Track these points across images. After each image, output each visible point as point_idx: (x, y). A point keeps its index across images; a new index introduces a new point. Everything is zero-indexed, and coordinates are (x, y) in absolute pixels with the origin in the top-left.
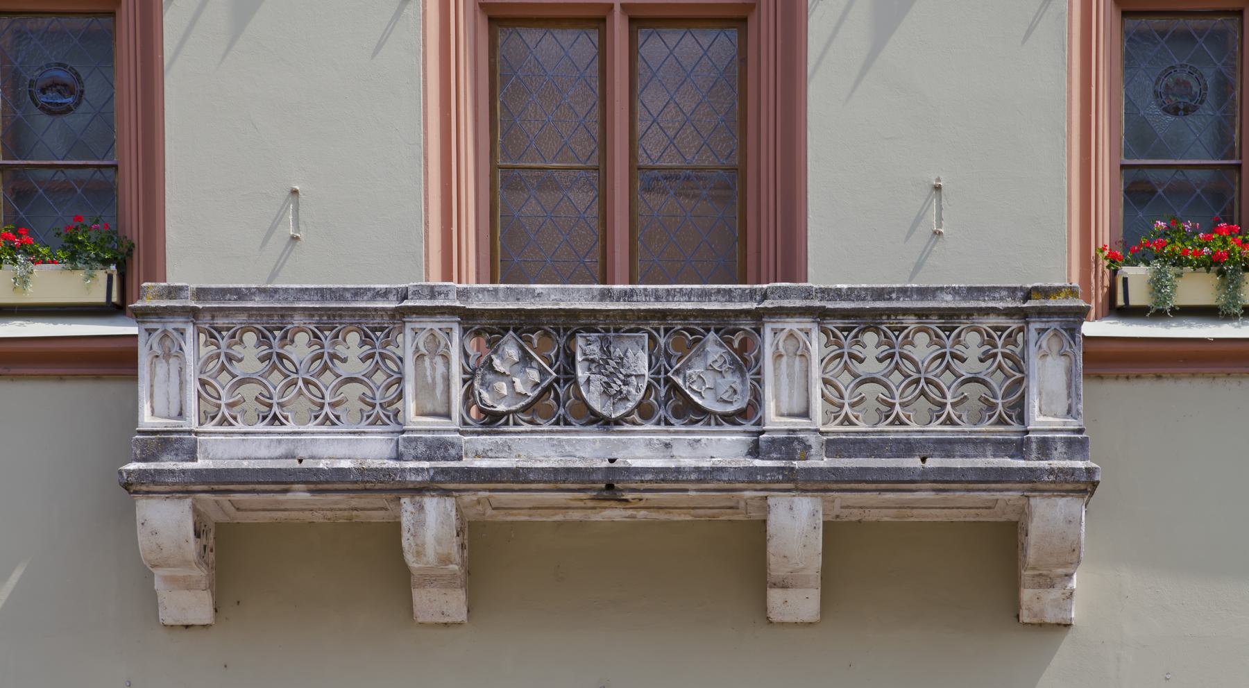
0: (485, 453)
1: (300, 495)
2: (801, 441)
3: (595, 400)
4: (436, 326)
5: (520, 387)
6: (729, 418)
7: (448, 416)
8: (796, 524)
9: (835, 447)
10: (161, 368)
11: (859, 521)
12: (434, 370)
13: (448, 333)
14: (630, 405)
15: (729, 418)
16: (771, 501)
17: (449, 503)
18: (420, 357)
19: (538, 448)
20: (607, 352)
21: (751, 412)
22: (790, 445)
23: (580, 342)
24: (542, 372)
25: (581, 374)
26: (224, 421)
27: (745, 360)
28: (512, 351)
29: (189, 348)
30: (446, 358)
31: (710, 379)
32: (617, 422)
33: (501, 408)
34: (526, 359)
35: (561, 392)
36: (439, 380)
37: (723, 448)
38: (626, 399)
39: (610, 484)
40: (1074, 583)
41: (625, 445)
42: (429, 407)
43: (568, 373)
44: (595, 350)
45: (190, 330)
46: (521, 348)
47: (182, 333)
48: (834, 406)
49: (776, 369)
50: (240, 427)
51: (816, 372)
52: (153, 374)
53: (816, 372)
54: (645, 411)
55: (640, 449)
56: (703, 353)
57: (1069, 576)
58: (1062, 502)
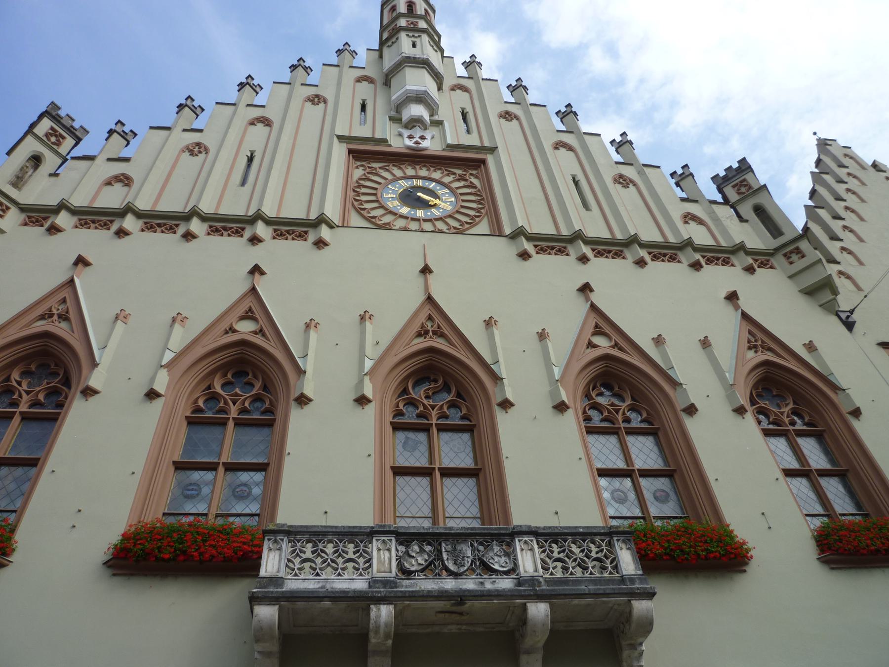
0: (407, 585)
1: (327, 604)
2: (537, 580)
3: (452, 567)
4: (386, 539)
5: (420, 560)
6: (505, 573)
7: (391, 572)
8: (539, 611)
9: (548, 581)
10: (272, 554)
11: (816, 249)
12: (384, 558)
13: (391, 540)
14: (466, 568)
15: (505, 573)
16: (528, 605)
17: (391, 607)
18: (379, 550)
19: (428, 585)
20: (455, 549)
21: (514, 570)
22: (533, 581)
23: (443, 545)
24: (429, 556)
25: (445, 556)
26: (296, 575)
27: (510, 554)
28: (416, 548)
29: (284, 546)
30: (389, 550)
31: (496, 559)
32: (461, 574)
33: (413, 569)
34: (422, 551)
35: (437, 564)
36: (387, 559)
37: (506, 584)
38: (463, 566)
39: (460, 597)
40: (644, 648)
41: (465, 584)
42: (382, 569)
43: (439, 557)
44: (449, 548)
45: (285, 539)
46: (420, 547)
47: (282, 540)
48: (546, 569)
49: (522, 554)
50: (302, 577)
51: (537, 555)
52: (268, 557)
53: (537, 555)
54: (471, 570)
55: (469, 584)
56: (492, 549)
57: (641, 644)
58: (644, 602)
